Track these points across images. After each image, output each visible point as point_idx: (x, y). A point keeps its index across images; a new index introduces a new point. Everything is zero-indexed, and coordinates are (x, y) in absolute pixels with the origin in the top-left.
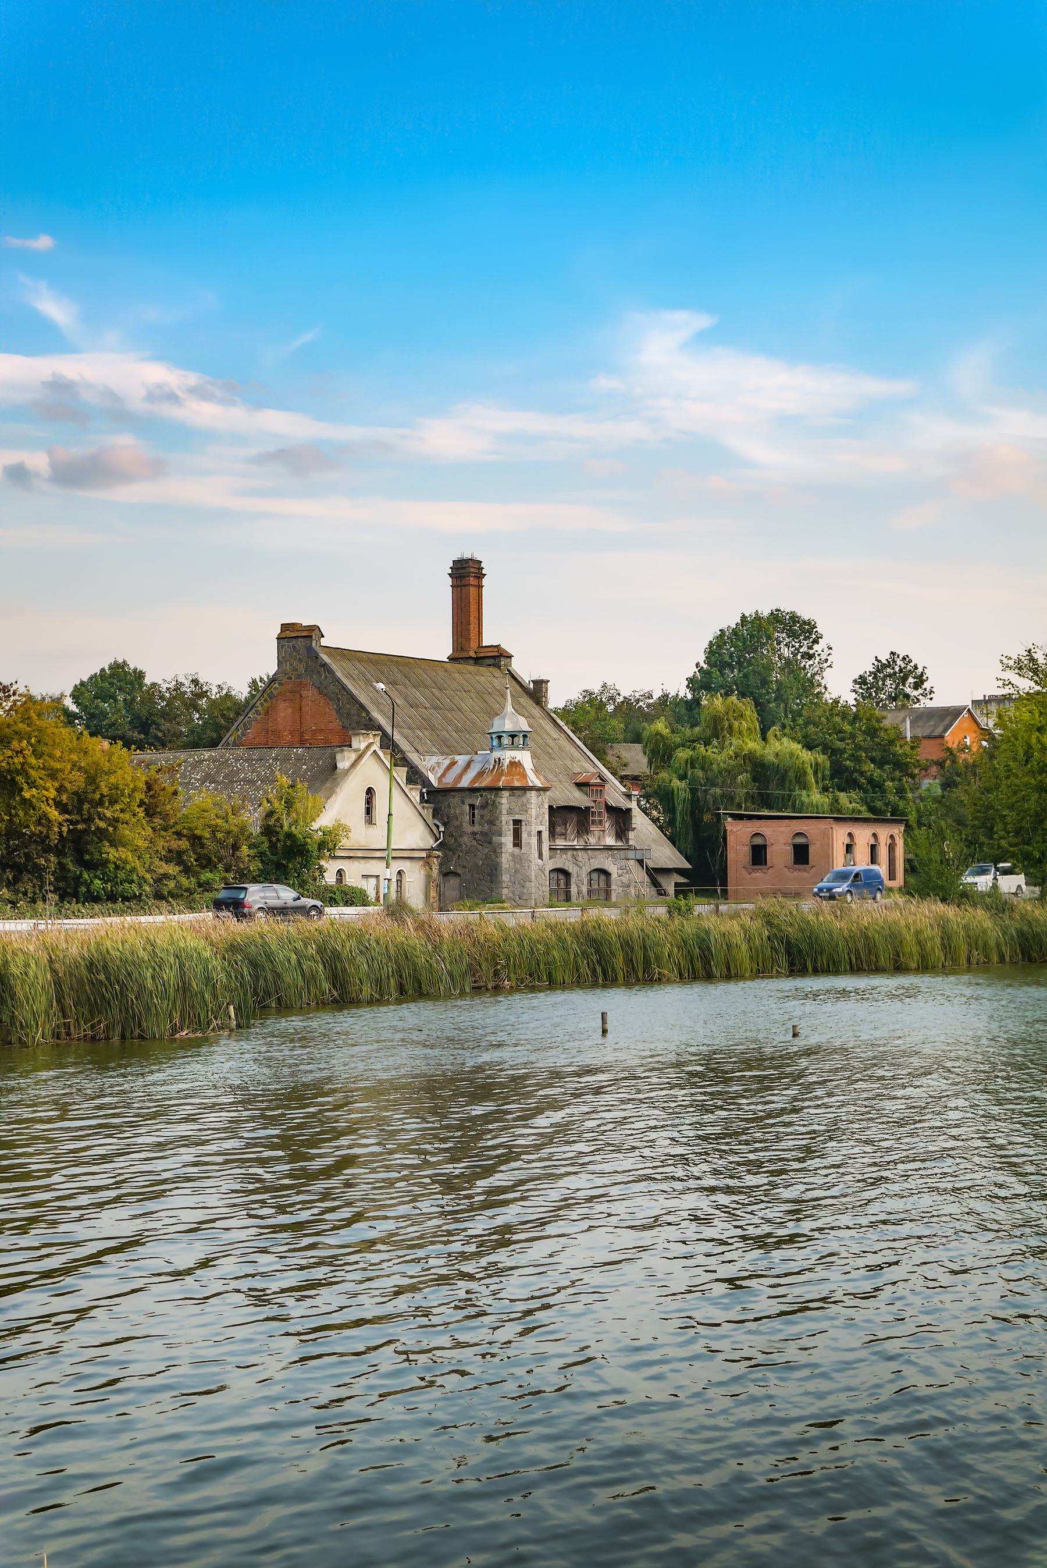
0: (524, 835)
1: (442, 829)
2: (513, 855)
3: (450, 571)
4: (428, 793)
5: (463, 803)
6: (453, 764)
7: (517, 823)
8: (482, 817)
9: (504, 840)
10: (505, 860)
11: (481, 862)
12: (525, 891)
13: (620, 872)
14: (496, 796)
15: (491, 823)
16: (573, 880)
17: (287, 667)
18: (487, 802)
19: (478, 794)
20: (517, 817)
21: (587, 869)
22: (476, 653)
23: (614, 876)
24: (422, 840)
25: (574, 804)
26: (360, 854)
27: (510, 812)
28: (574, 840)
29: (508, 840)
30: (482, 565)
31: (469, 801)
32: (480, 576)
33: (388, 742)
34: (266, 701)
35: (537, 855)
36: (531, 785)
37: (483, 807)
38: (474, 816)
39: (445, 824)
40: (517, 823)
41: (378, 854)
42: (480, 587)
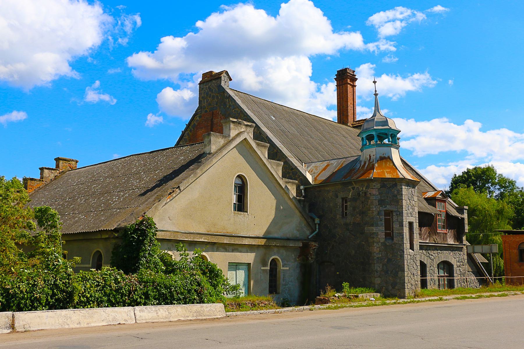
0: (396, 226)
1: (317, 221)
2: (384, 244)
3: (336, 77)
4: (305, 189)
5: (337, 197)
6: (328, 165)
7: (388, 213)
8: (354, 209)
9: (374, 229)
10: (376, 249)
11: (353, 252)
12: (398, 281)
13: (458, 263)
14: (368, 187)
15: (363, 213)
16: (428, 269)
17: (205, 104)
18: (359, 194)
19: (350, 187)
20: (389, 208)
21: (437, 261)
22: (352, 124)
23: (455, 266)
24: (298, 230)
25: (426, 211)
26: (226, 241)
27: (381, 202)
28: (426, 239)
29: (380, 231)
30: (355, 73)
31: (341, 195)
32: (354, 79)
33: (259, 135)
34: (191, 131)
35: (408, 246)
36: (401, 177)
37: (354, 199)
38: (346, 209)
39: (320, 217)
40: (388, 213)
41: (246, 242)
42: (354, 86)
